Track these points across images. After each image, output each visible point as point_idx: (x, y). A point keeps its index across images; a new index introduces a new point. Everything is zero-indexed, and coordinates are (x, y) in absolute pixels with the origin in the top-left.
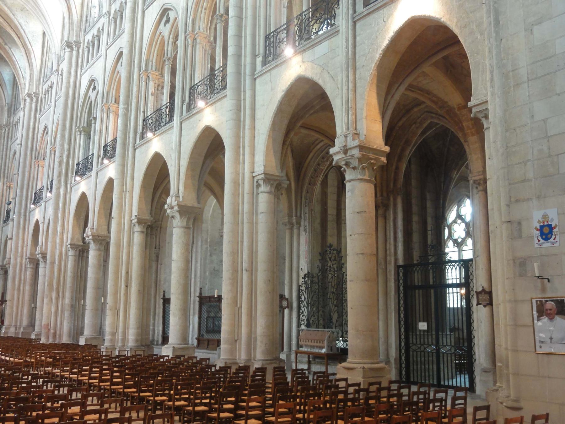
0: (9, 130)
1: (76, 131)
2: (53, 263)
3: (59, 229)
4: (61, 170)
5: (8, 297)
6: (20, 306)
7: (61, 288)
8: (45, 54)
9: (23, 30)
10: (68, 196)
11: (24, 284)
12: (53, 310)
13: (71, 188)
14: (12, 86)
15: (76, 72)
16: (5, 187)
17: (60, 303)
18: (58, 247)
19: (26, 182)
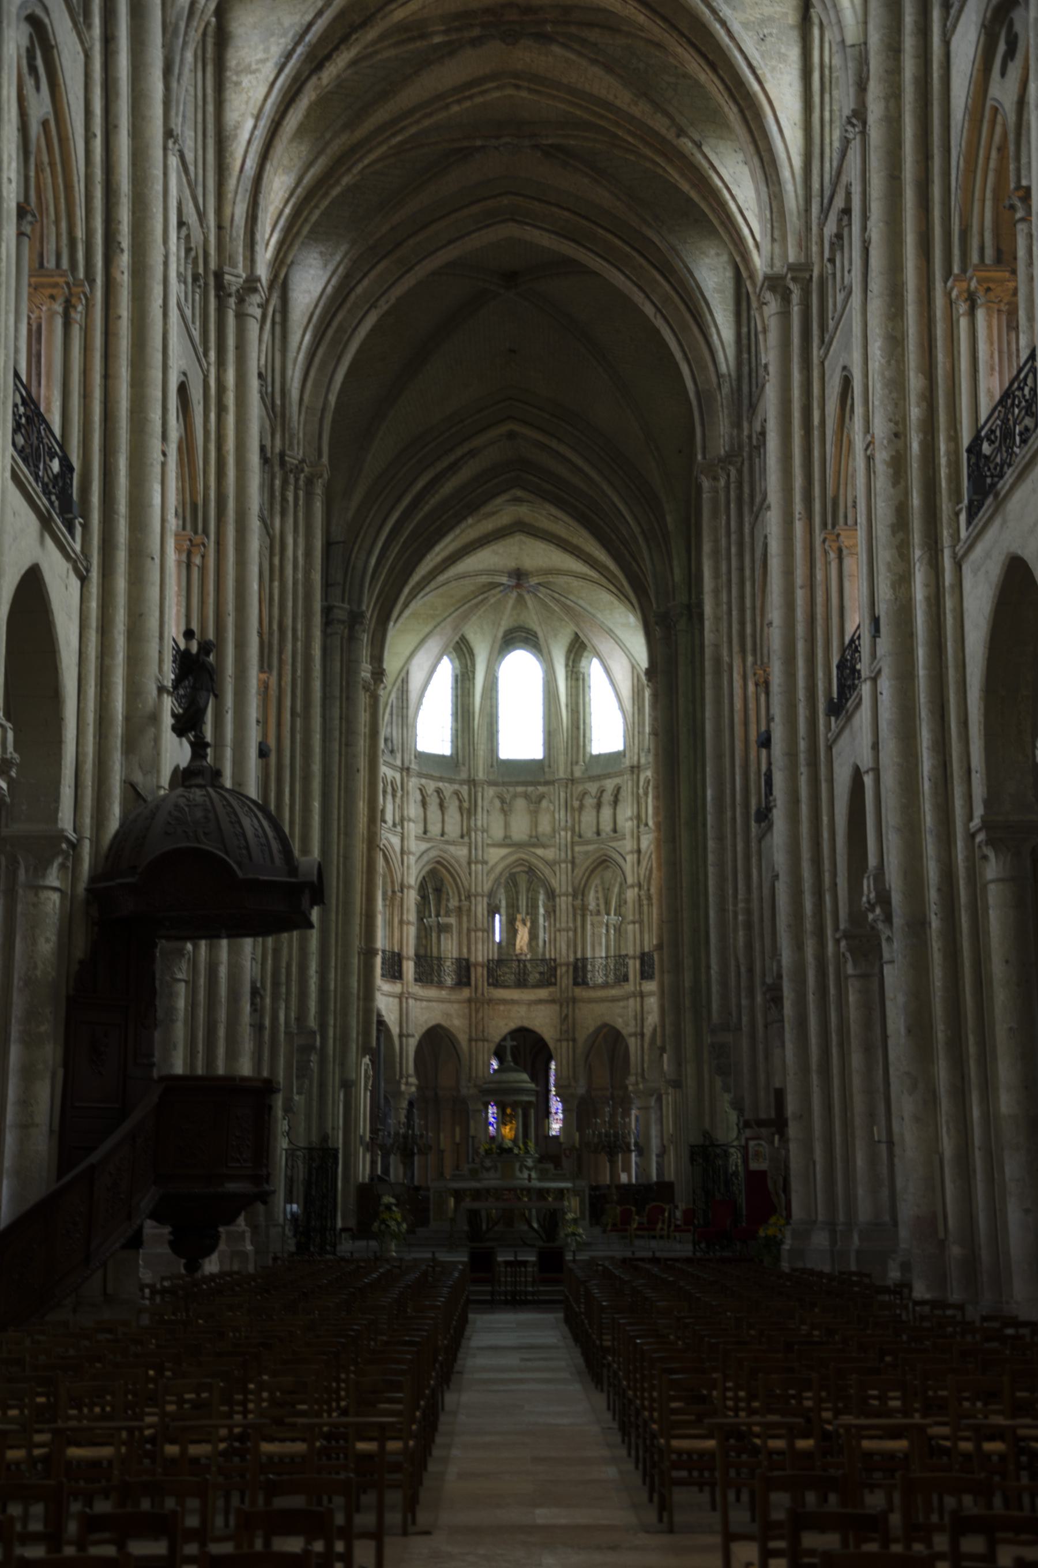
0: (740, 472)
1: (950, 303)
2: (918, 925)
3: (927, 764)
4: (906, 493)
5: (791, 1107)
6: (838, 1139)
7: (971, 1039)
8: (817, 99)
9: (723, 23)
10: (949, 604)
11: (841, 1045)
12: (948, 1146)
13: (958, 566)
14: (731, 307)
15: (924, 31)
16: (751, 688)
17: (976, 1113)
18: (930, 848)
19: (800, 629)
